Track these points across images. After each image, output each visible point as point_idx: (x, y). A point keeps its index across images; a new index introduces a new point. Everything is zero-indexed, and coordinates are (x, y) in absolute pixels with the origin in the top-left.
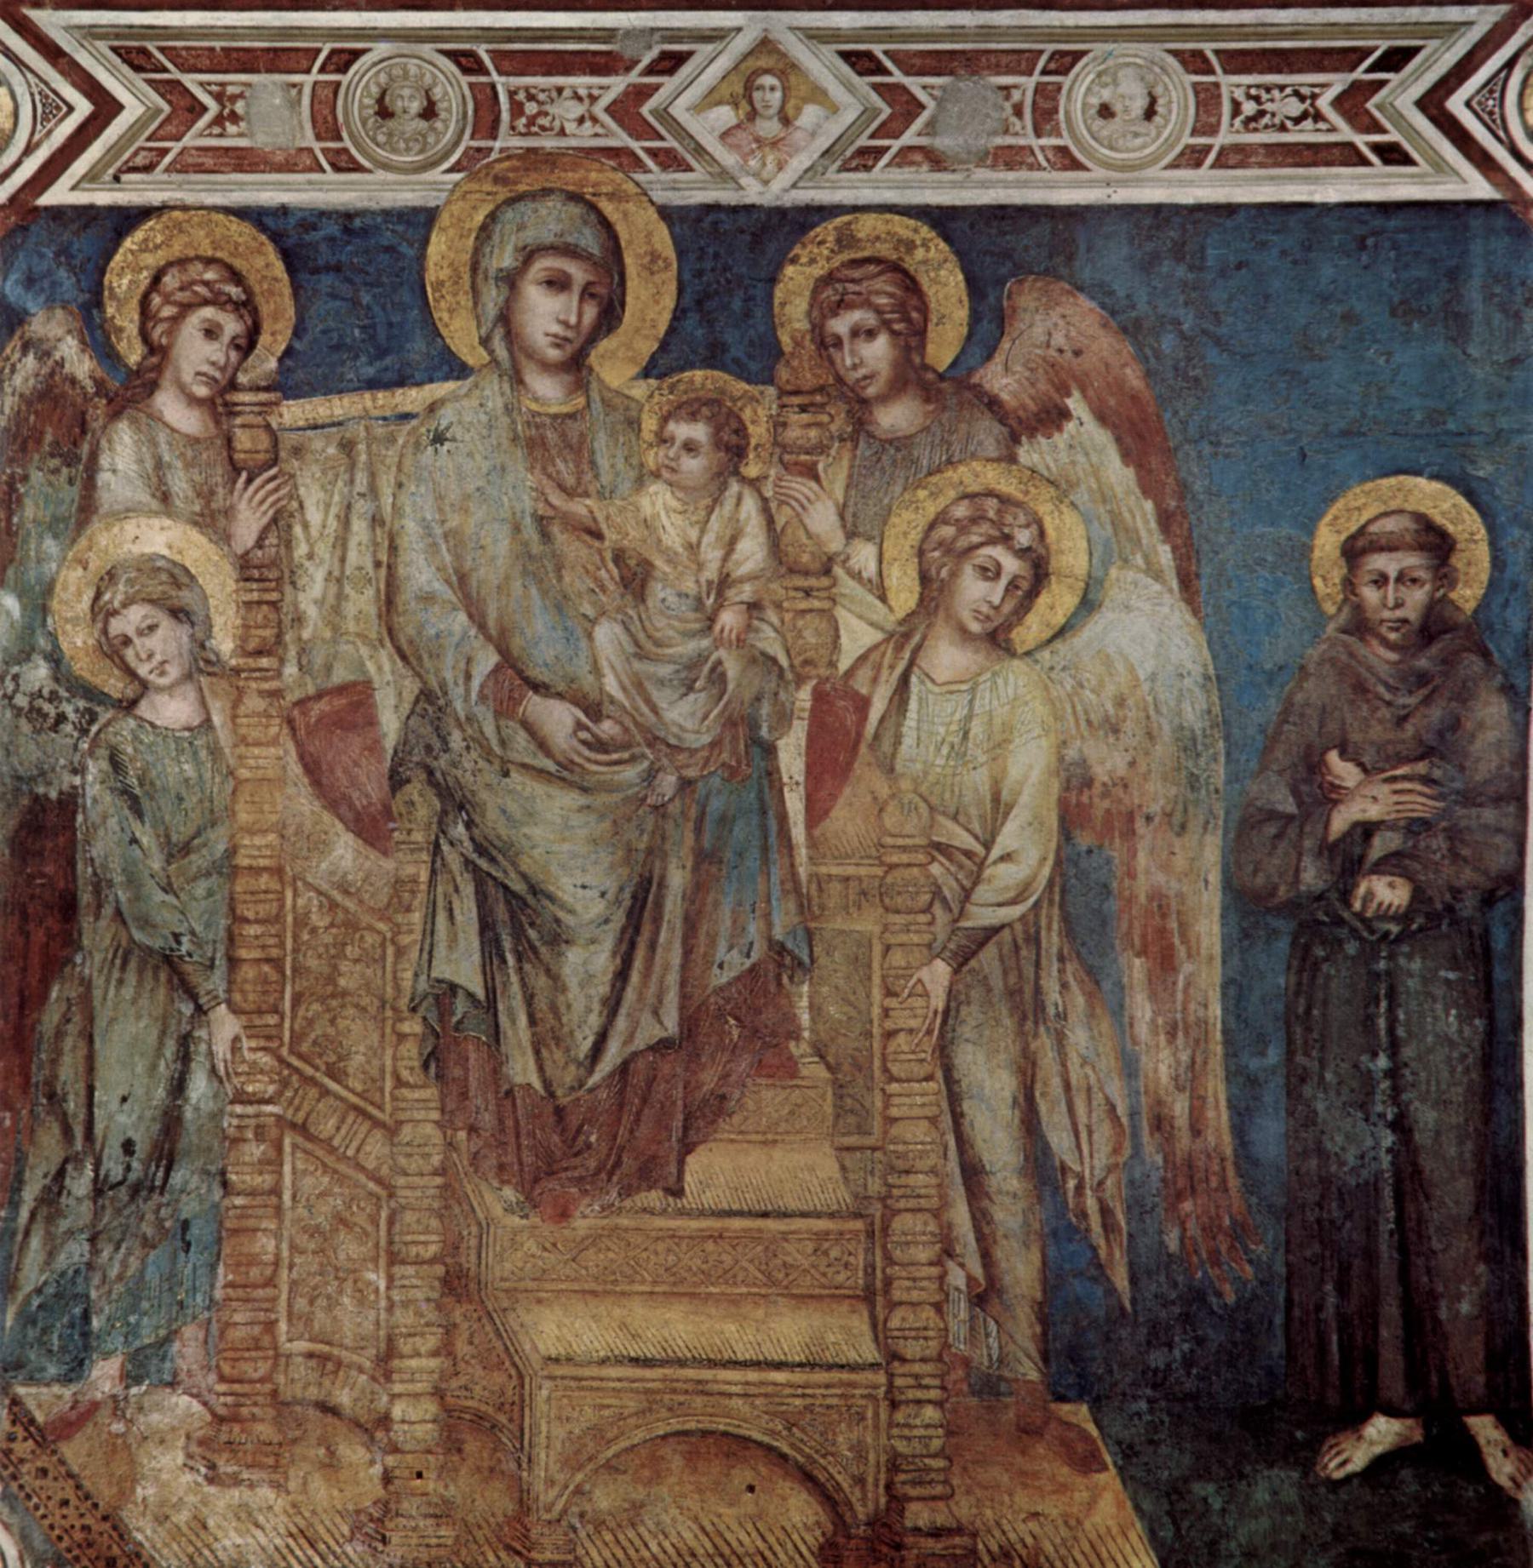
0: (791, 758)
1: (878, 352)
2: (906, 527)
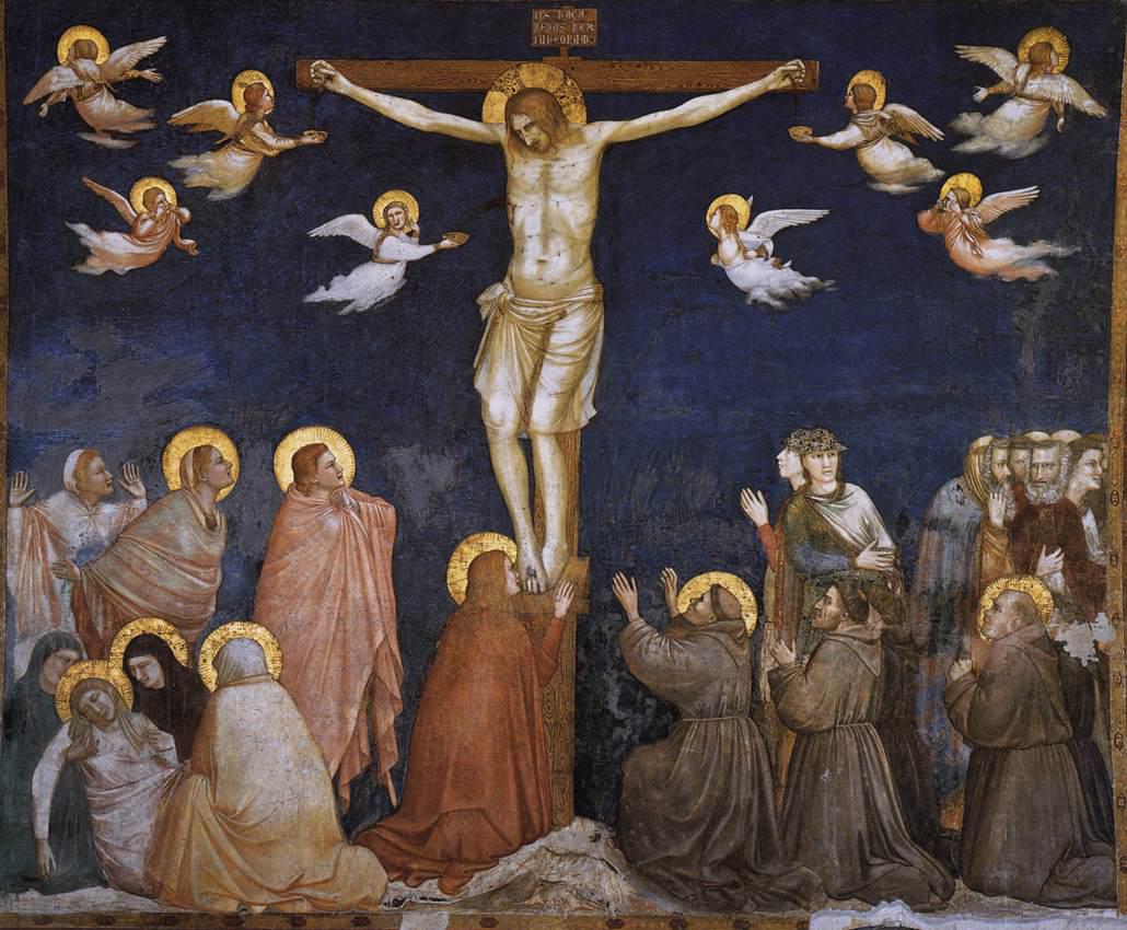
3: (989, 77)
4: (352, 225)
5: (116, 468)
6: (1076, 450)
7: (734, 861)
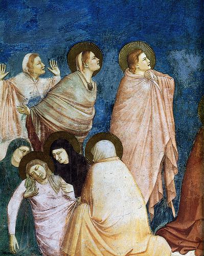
5: (46, 61)
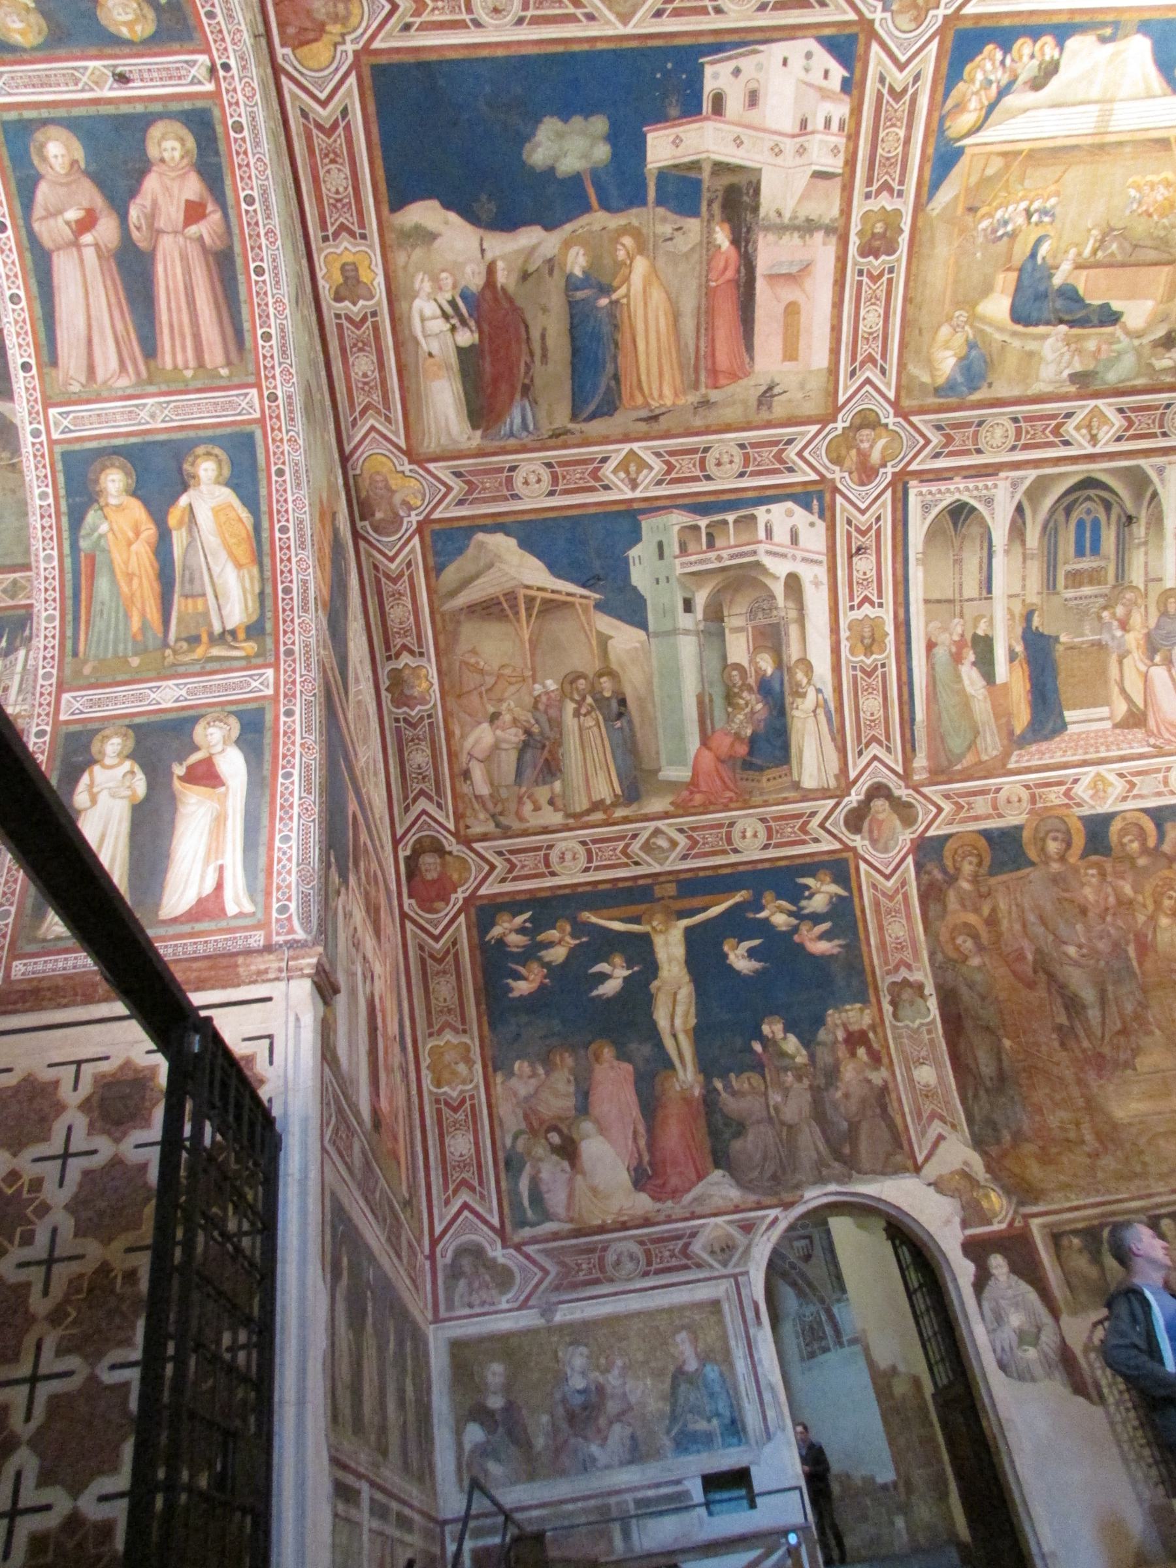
0: (1131, 951)
1: (1135, 845)
2: (1148, 888)
3: (807, 887)
4: (603, 967)
5: (532, 1065)
6: (862, 1010)
7: (774, 1177)
